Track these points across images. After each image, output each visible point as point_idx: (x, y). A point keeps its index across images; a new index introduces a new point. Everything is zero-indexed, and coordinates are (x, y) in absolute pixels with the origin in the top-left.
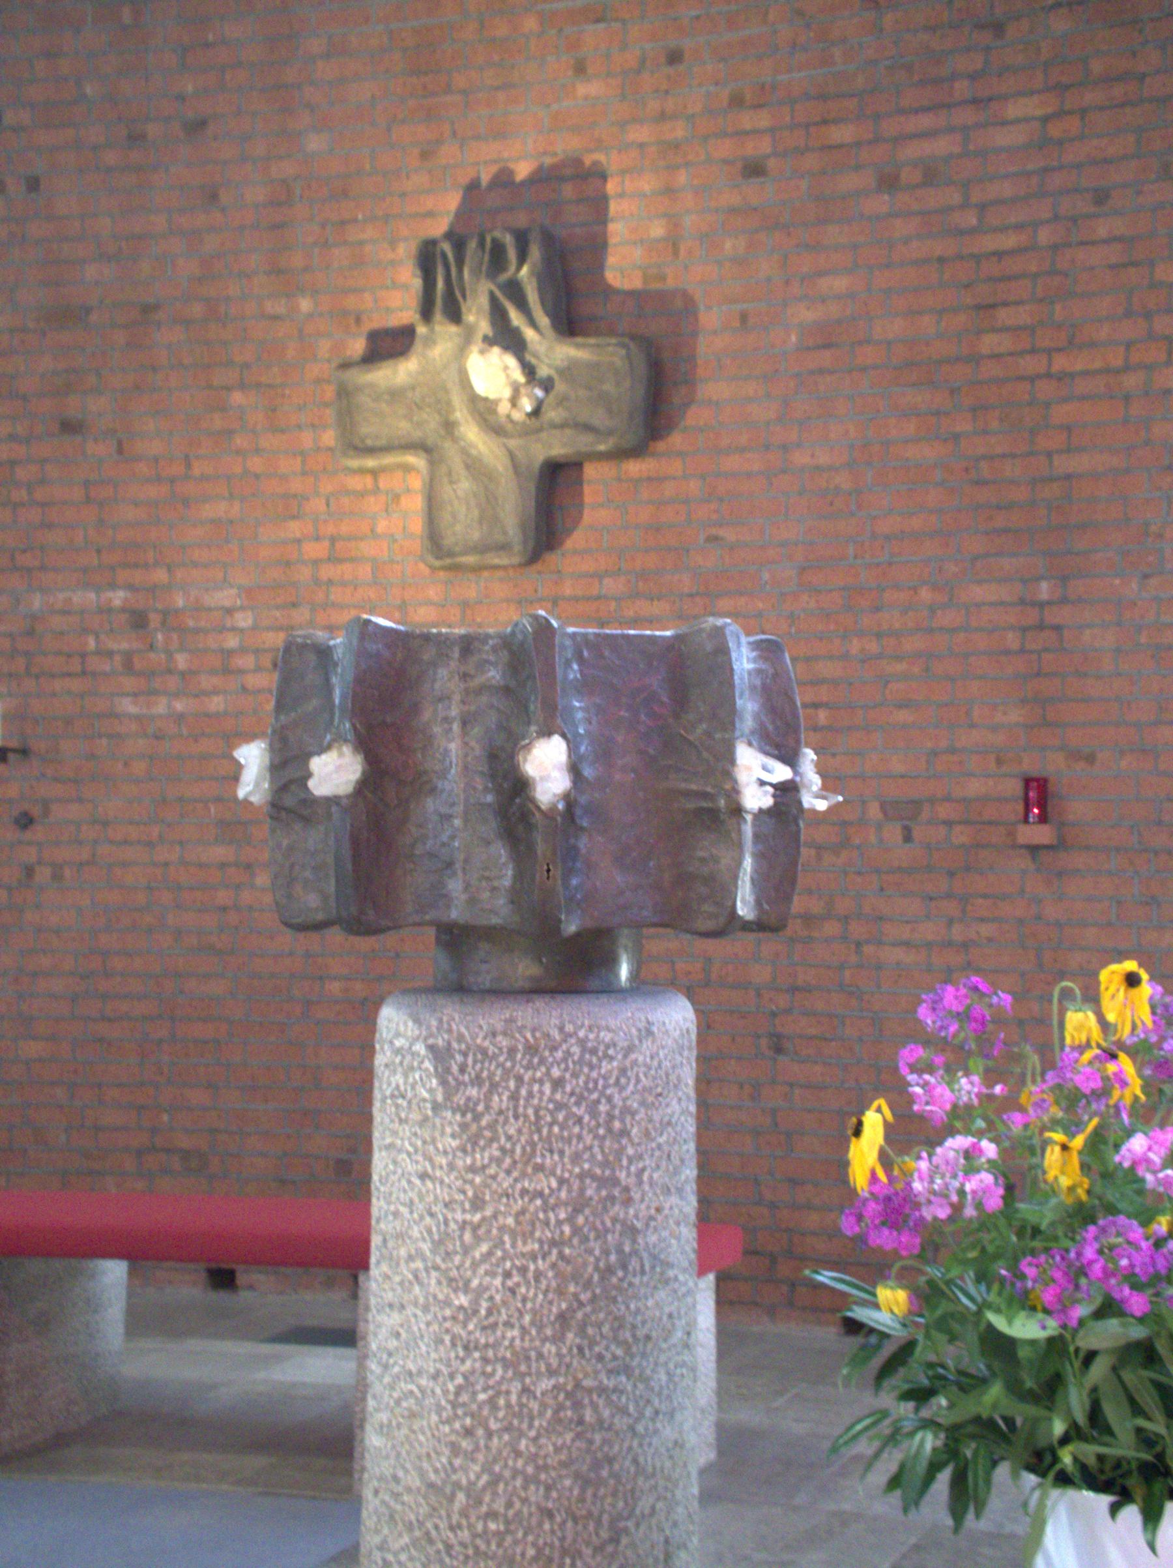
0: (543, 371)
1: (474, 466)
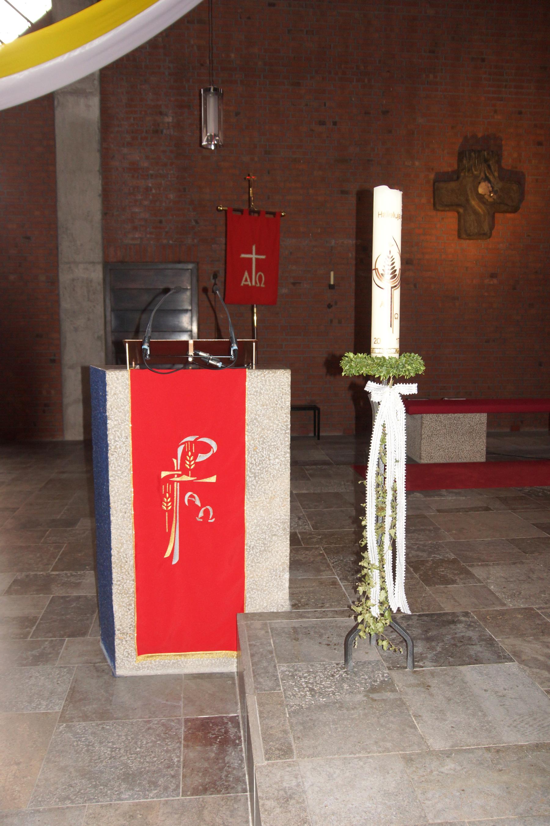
0: (495, 189)
1: (475, 213)
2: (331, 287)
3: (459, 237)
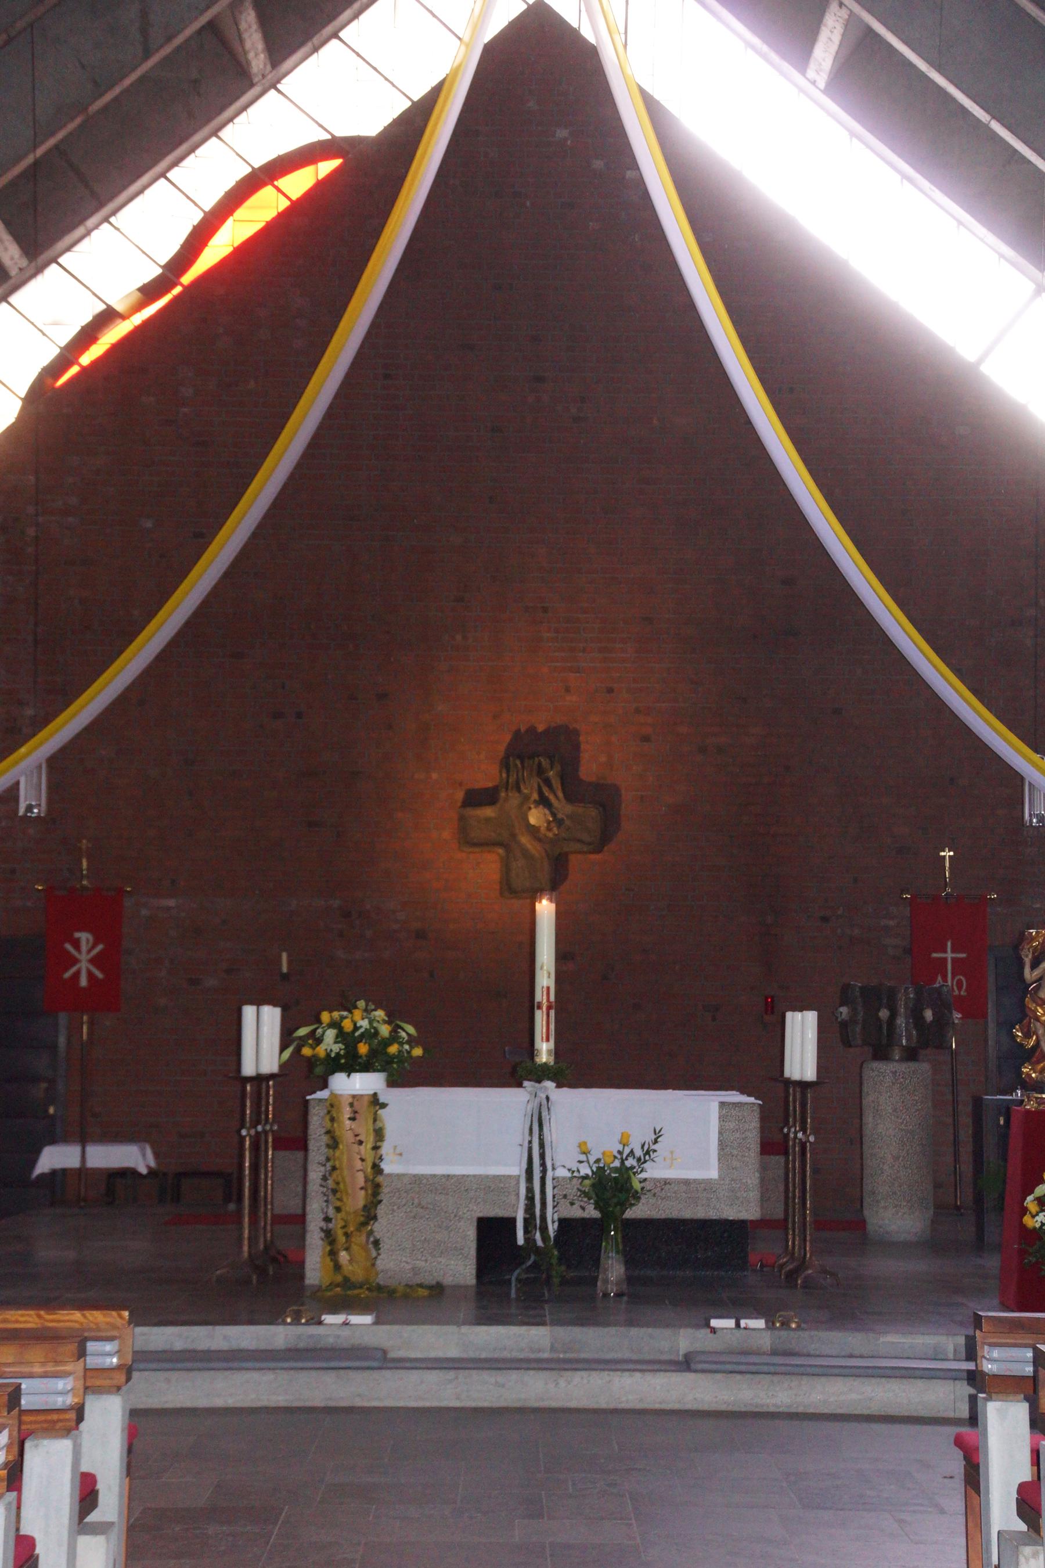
0: (560, 816)
1: (526, 854)
2: (285, 977)
3: (501, 894)
